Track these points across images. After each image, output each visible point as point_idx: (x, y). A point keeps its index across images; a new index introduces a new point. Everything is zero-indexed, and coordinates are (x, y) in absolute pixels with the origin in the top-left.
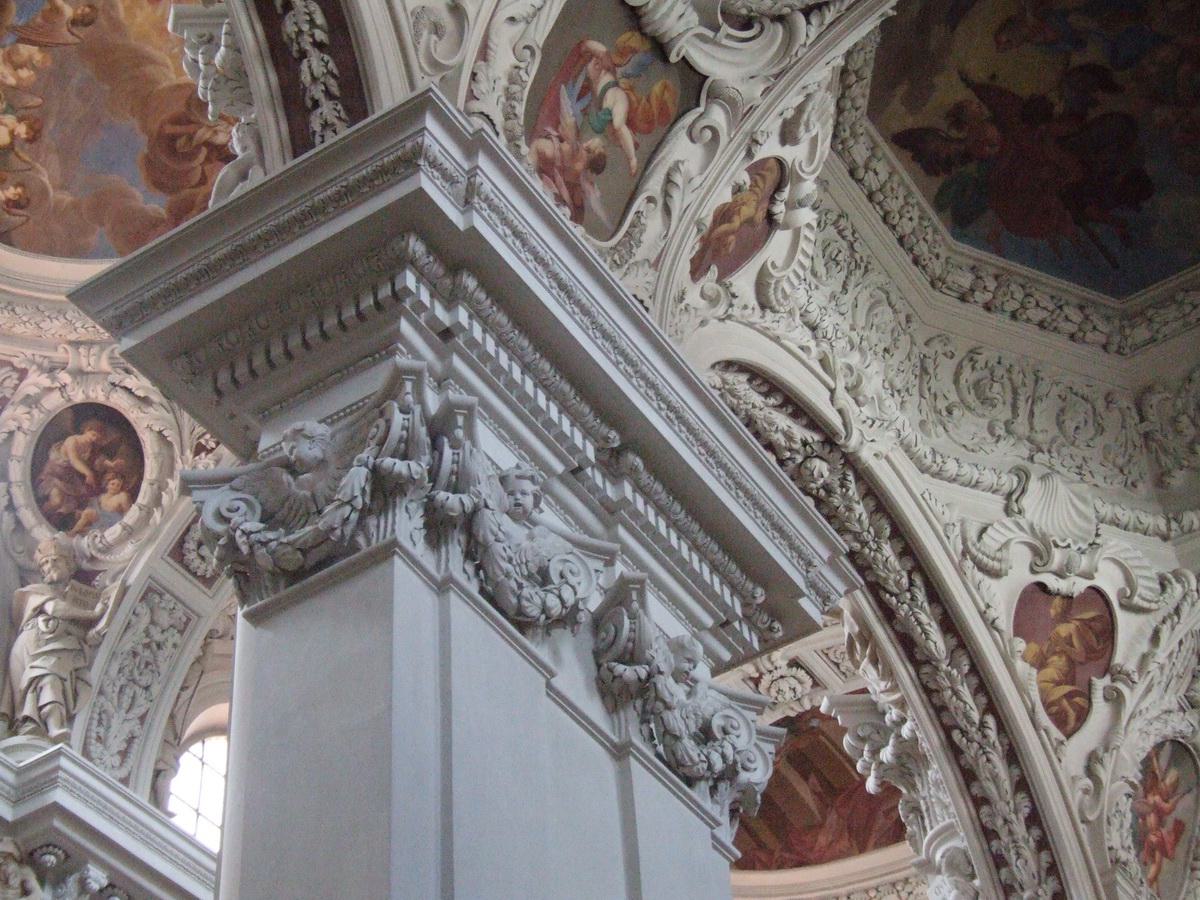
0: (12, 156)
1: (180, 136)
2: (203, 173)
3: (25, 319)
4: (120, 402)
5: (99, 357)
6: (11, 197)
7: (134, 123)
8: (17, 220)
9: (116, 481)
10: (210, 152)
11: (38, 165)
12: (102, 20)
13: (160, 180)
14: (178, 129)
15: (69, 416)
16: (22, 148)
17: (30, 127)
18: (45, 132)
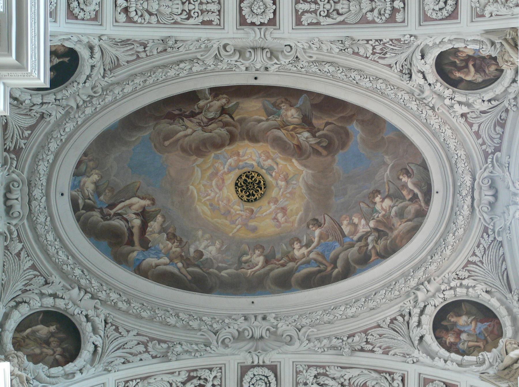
0: (391, 191)
1: (322, 146)
2: (325, 127)
3: (443, 134)
4: (432, 76)
5: (427, 96)
6: (406, 177)
7: (335, 166)
8: (412, 166)
9: (459, 55)
10: (316, 132)
11: (385, 180)
12: (310, 217)
13: (344, 137)
14: (320, 149)
15: (460, 86)
16: (385, 191)
17: (374, 198)
18: (371, 190)
